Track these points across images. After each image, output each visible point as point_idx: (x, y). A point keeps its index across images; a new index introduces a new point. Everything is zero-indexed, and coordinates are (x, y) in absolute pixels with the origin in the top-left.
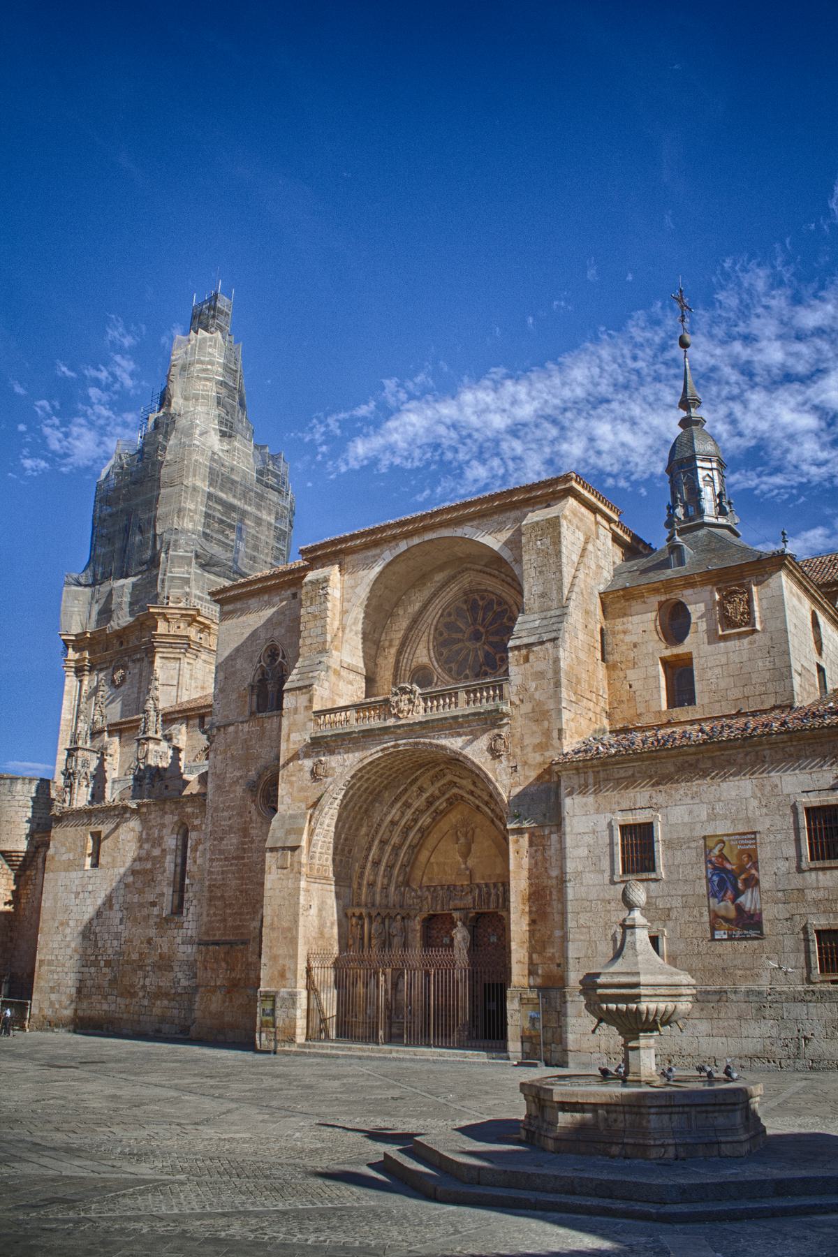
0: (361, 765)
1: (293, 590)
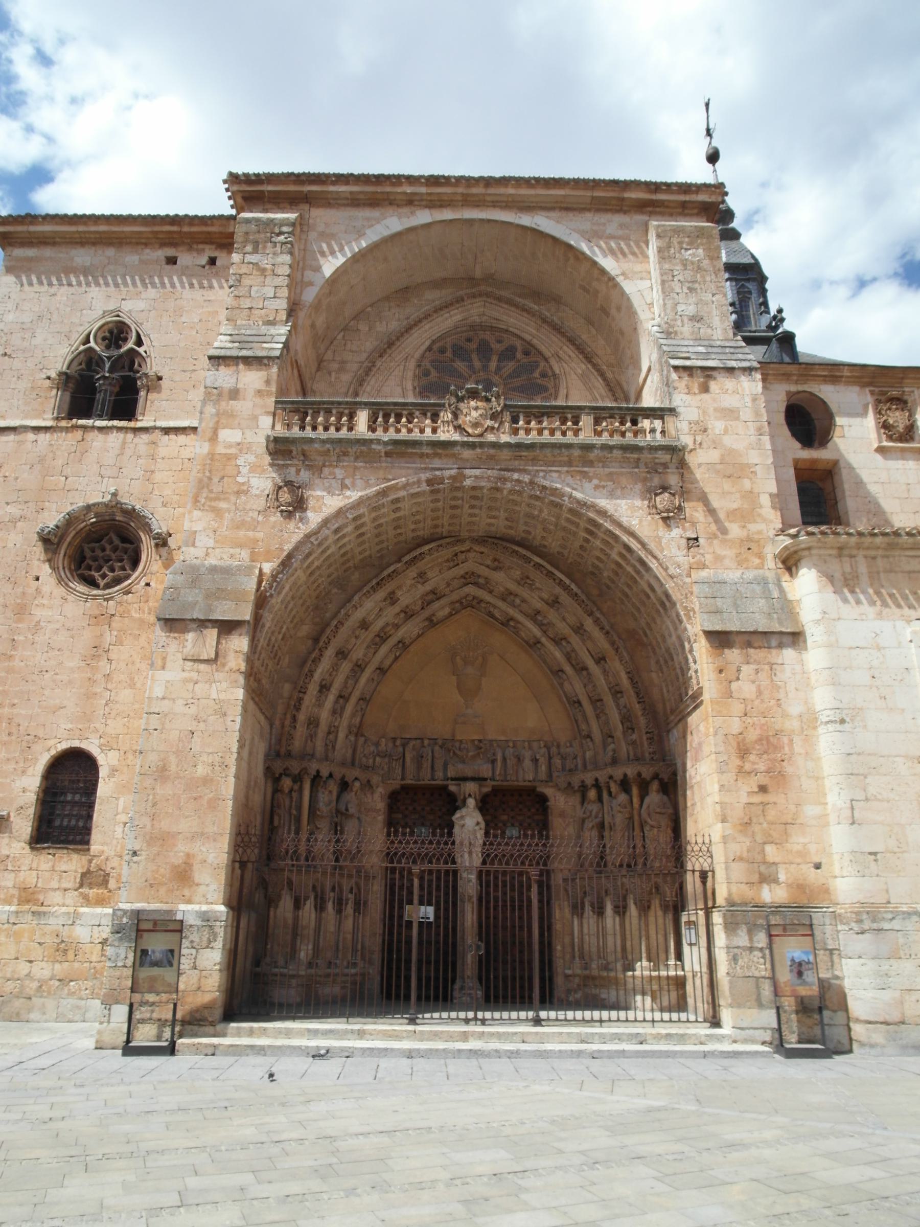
1: (170, 252)
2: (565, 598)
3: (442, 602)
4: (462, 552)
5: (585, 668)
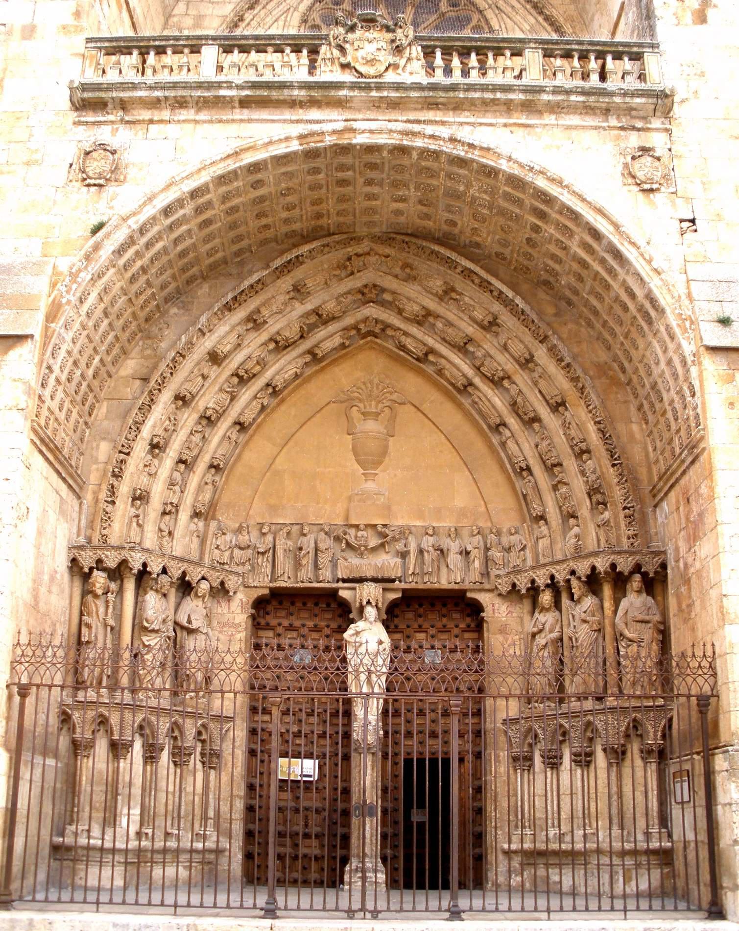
0: (232, 165)
2: (507, 319)
3: (332, 327)
4: (358, 255)
5: (536, 419)
